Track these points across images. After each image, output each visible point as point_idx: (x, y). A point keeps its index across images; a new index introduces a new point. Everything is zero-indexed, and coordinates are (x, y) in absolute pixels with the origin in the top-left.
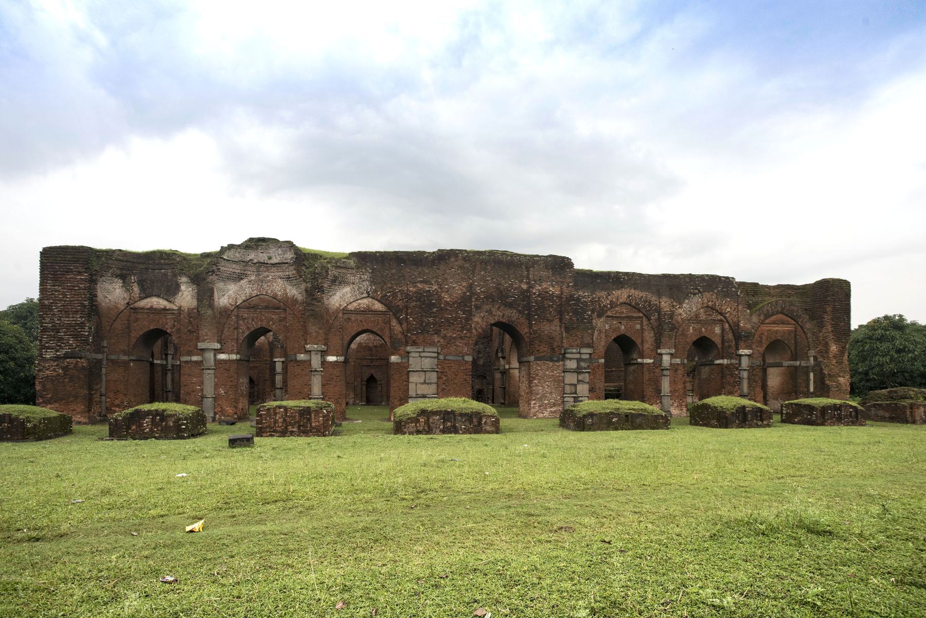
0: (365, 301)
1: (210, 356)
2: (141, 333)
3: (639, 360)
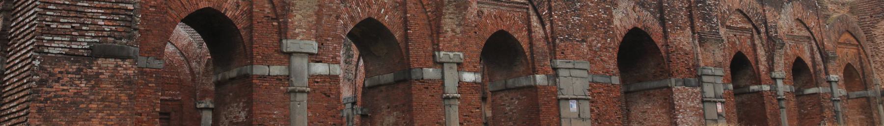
1: (299, 63)
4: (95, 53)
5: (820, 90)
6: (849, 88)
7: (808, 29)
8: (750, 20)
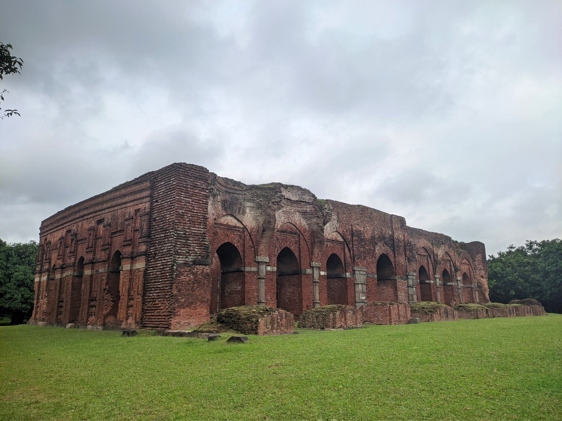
0: (335, 234)
2: (219, 245)
3: (427, 281)
4: (195, 263)
5: (453, 284)
6: (464, 283)
7: (450, 256)
8: (427, 252)
